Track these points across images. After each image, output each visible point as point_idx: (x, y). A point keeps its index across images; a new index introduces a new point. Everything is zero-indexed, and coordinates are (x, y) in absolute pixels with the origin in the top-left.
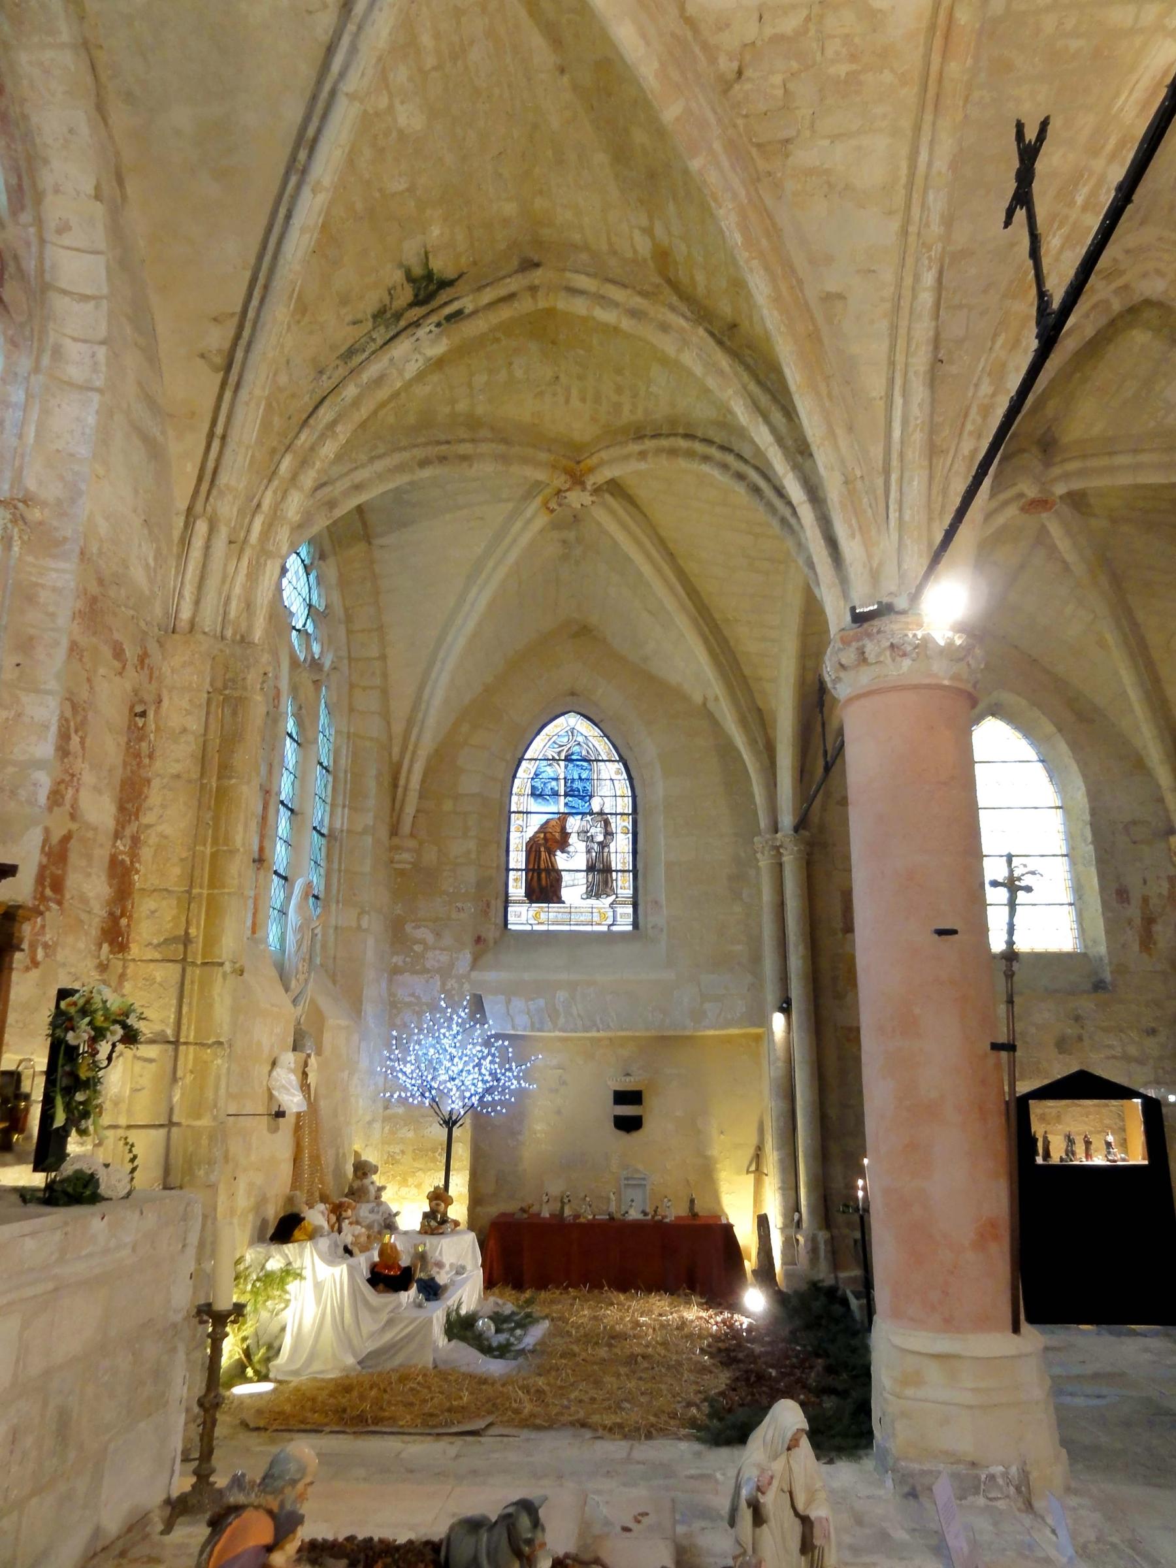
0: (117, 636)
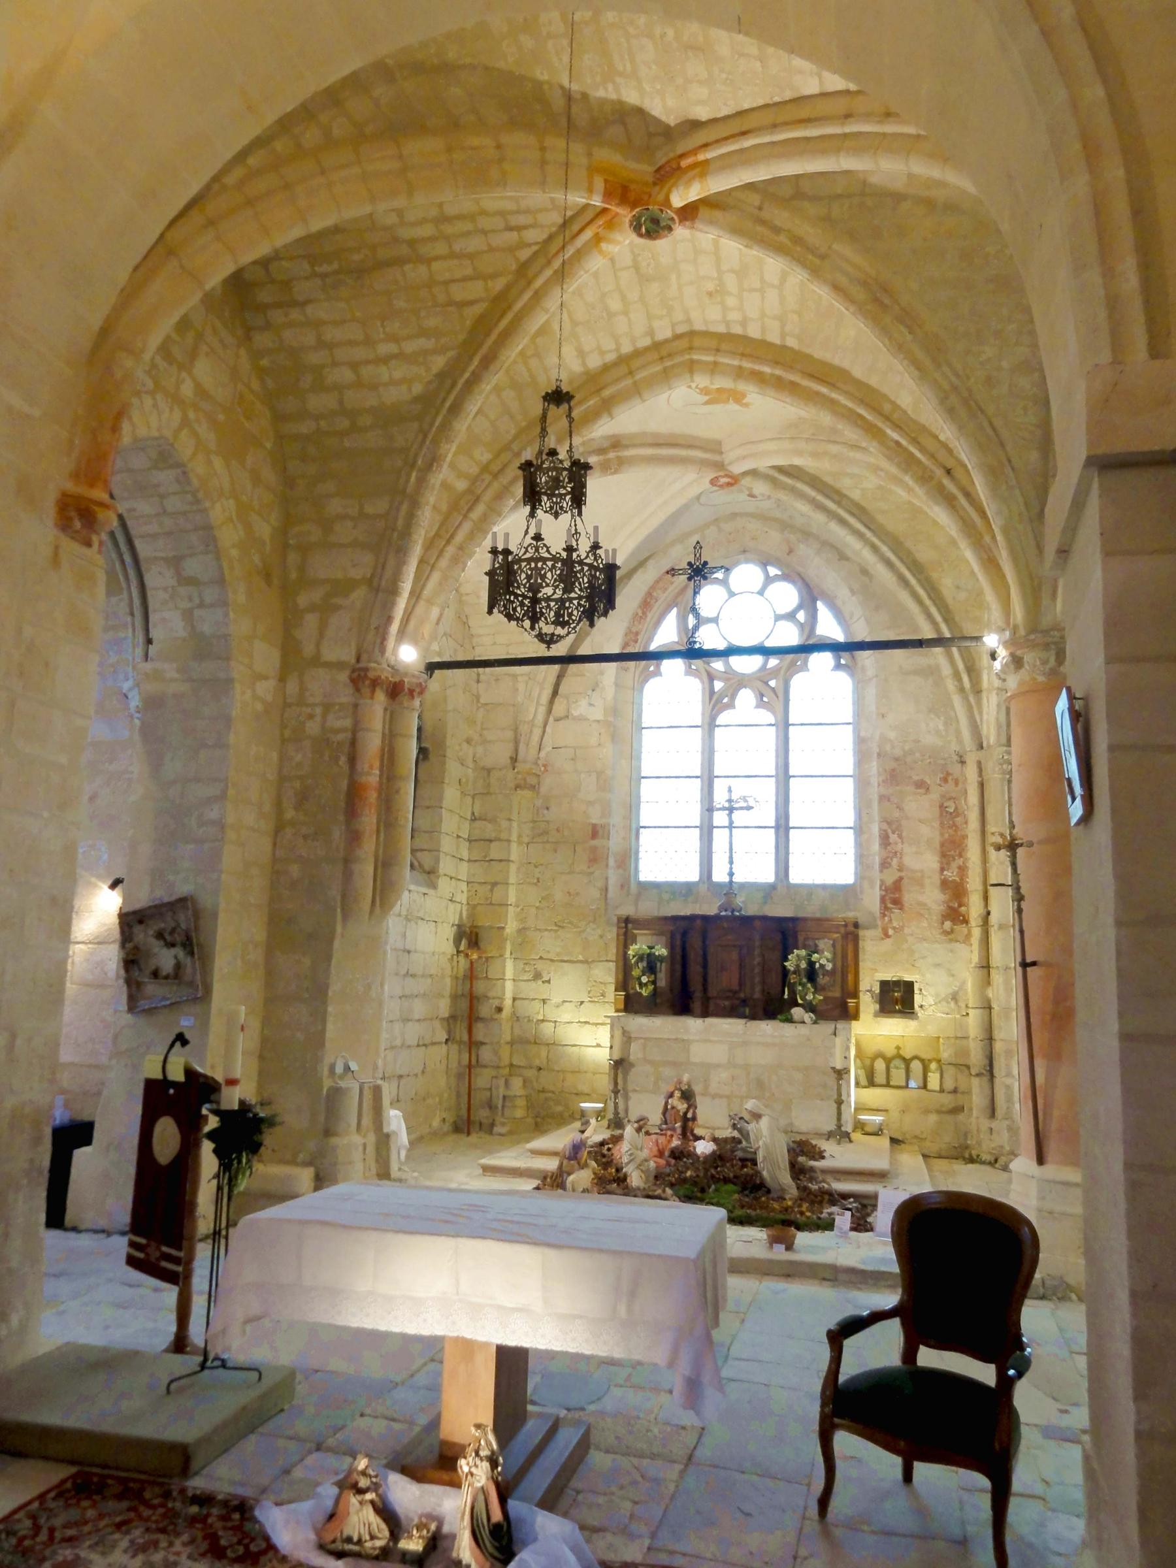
0: (916, 778)
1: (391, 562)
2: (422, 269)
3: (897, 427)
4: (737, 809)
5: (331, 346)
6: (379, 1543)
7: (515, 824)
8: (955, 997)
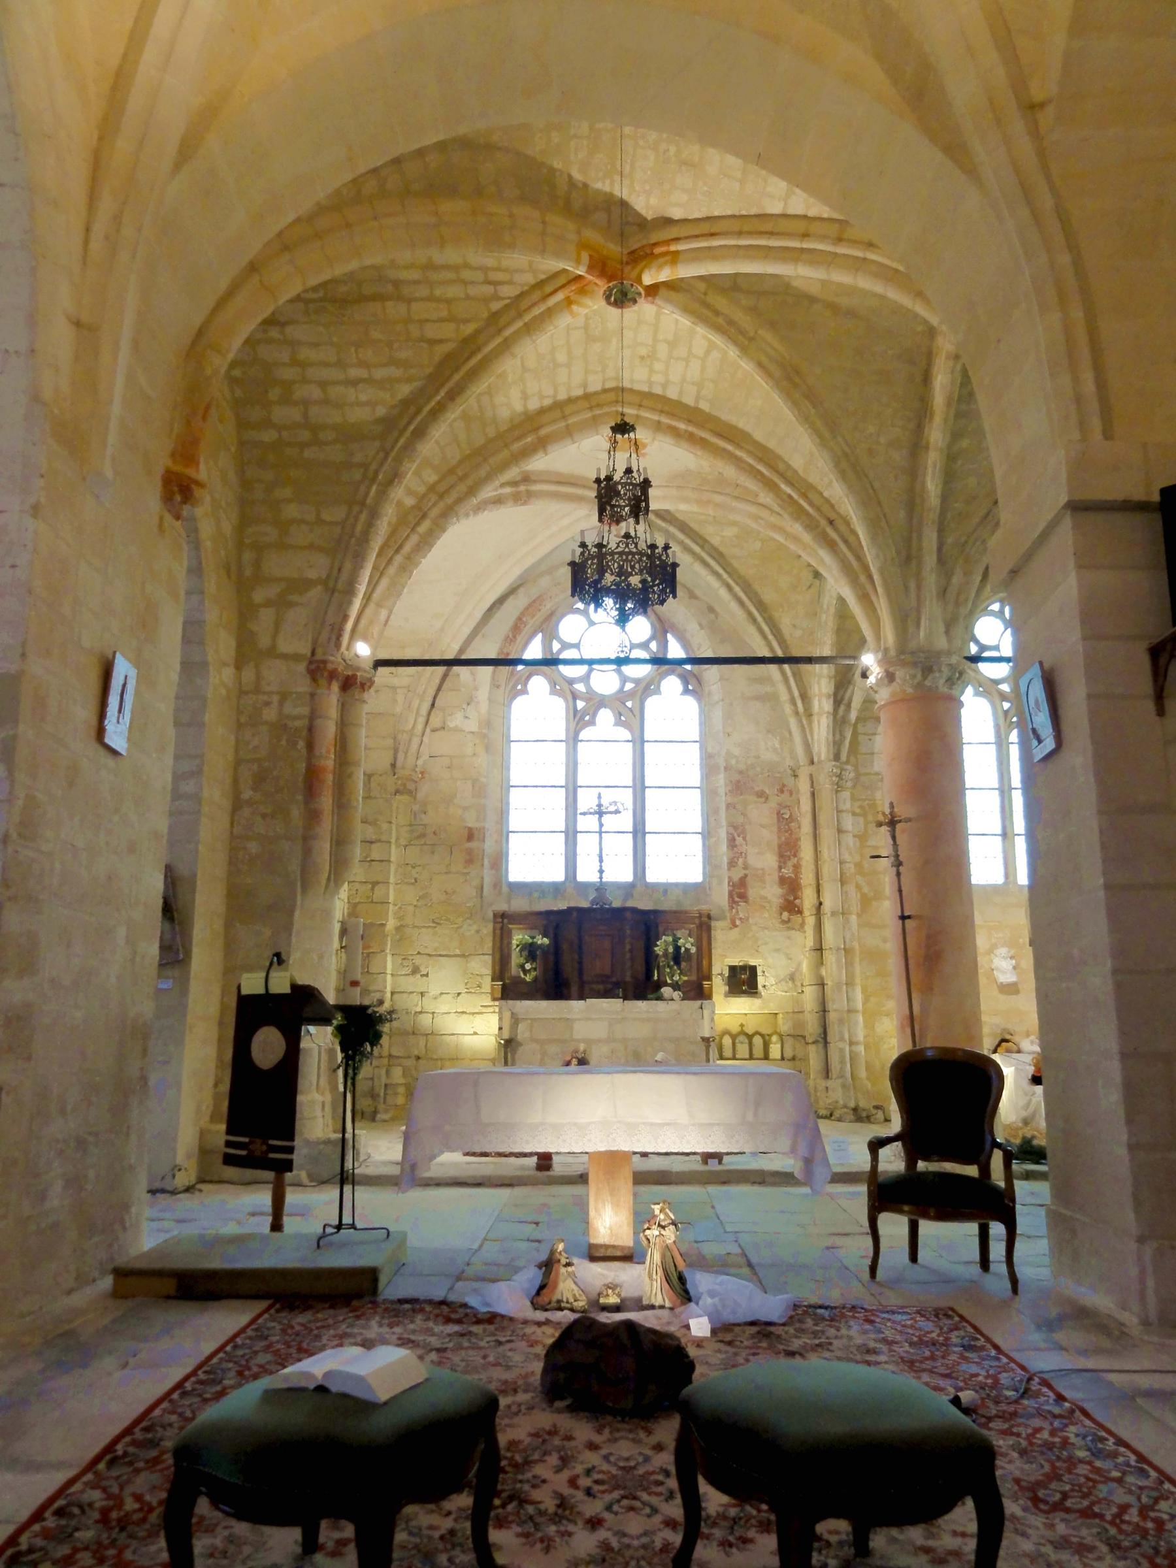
0: (757, 789)
1: (348, 565)
2: (402, 308)
3: (790, 483)
4: (606, 813)
5: (303, 365)
6: (581, 1304)
7: (394, 827)
8: (792, 978)
